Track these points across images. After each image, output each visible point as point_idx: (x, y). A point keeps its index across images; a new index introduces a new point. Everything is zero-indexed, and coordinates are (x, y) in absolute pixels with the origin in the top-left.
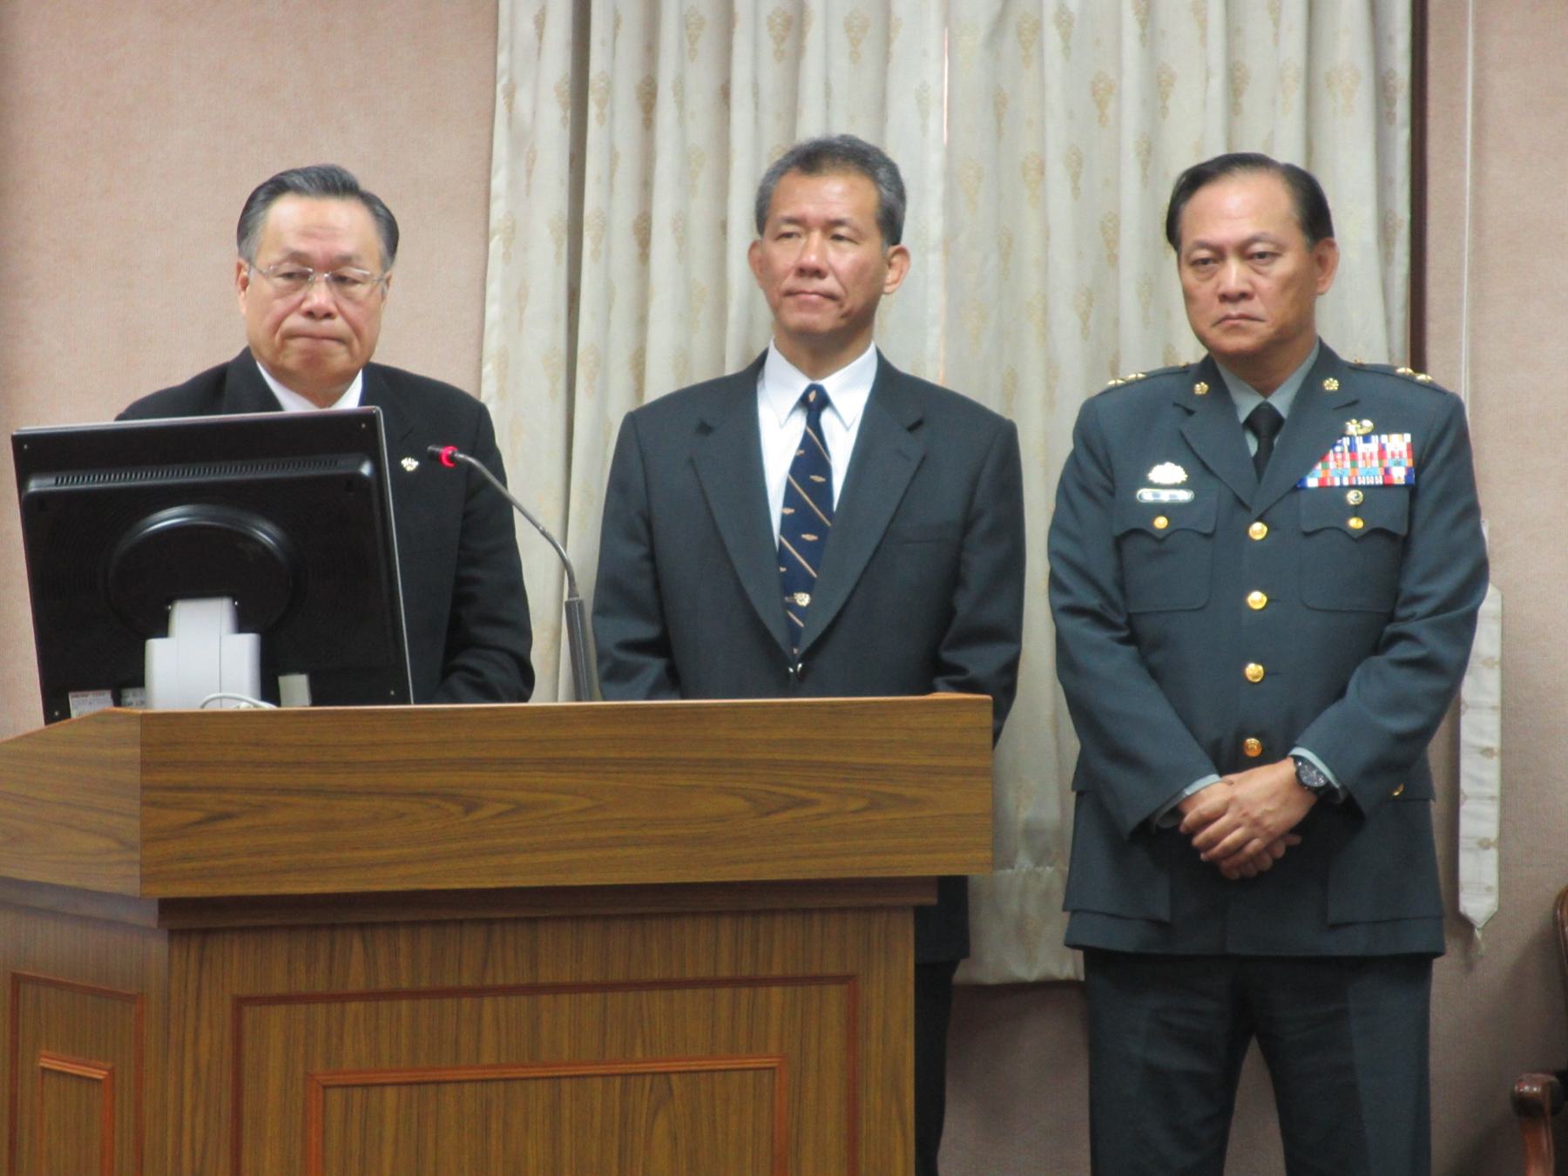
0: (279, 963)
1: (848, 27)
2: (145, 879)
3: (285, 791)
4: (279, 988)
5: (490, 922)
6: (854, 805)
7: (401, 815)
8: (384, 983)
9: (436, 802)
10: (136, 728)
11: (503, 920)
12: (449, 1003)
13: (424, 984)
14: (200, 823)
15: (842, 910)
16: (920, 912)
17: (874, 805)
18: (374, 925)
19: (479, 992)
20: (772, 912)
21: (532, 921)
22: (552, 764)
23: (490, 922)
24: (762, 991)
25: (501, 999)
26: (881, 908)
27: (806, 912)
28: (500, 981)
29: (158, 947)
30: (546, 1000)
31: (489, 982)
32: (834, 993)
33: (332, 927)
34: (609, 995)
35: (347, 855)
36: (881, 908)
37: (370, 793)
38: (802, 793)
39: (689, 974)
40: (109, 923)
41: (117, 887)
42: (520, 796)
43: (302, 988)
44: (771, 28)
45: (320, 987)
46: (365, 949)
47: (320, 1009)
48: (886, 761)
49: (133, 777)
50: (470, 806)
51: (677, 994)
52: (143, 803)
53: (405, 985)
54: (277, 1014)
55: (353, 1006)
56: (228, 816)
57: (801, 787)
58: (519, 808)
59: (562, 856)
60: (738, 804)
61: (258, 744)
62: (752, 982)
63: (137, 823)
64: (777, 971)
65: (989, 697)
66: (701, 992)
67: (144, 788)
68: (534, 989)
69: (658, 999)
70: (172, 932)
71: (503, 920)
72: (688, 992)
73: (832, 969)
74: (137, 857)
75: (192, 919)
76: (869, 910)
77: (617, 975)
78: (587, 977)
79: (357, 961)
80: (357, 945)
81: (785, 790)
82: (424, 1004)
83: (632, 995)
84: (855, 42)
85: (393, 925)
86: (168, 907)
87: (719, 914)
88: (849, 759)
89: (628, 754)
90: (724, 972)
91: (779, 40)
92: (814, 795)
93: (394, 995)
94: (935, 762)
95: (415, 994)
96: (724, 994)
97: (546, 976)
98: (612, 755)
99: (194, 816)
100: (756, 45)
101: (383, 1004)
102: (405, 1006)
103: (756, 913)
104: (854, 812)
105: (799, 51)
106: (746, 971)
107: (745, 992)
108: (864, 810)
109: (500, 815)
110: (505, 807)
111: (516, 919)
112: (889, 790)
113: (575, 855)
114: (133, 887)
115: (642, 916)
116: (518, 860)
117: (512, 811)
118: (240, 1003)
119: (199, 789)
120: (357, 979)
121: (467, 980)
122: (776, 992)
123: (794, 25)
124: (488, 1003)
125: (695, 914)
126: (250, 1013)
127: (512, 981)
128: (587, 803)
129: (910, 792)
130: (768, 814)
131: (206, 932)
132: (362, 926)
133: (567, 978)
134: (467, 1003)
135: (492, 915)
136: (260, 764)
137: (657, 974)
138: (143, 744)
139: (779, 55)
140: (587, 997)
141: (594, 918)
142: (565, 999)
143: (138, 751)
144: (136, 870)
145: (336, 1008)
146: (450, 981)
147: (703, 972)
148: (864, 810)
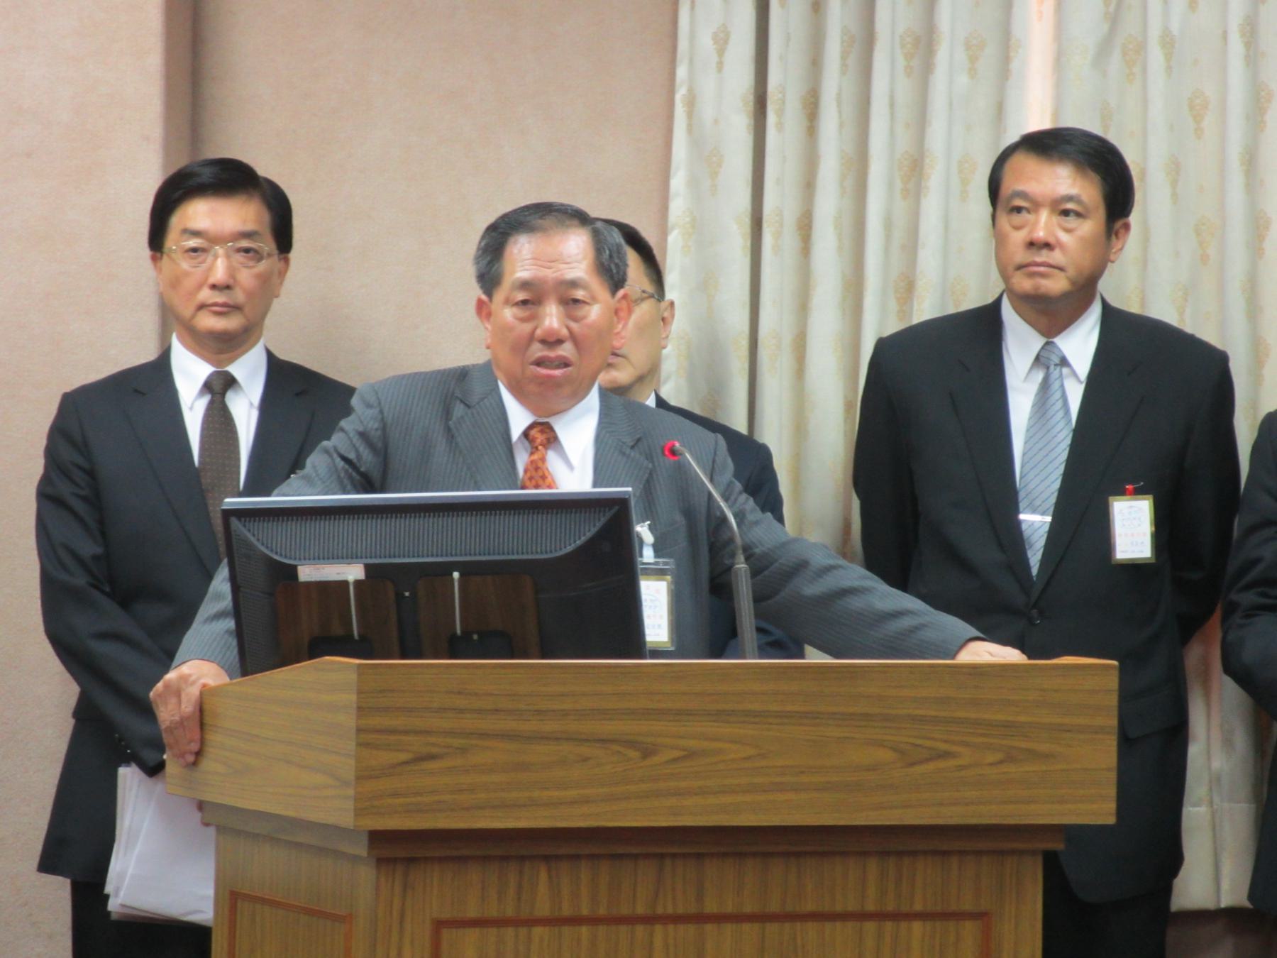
0: (473, 891)
1: (968, 46)
2: (359, 813)
3: (484, 735)
4: (472, 912)
5: (662, 856)
6: (991, 758)
7: (586, 759)
8: (566, 911)
9: (615, 747)
10: (353, 677)
11: (674, 856)
12: (624, 929)
13: (602, 911)
14: (406, 763)
15: (979, 853)
16: (1051, 862)
17: (1010, 758)
18: (558, 858)
19: (650, 920)
20: (914, 854)
21: (699, 856)
22: (721, 716)
23: (662, 856)
24: (904, 925)
25: (671, 927)
26: (1013, 852)
27: (945, 853)
28: (670, 910)
29: (366, 875)
30: (709, 927)
31: (660, 911)
32: (969, 929)
33: (522, 859)
34: (768, 925)
35: (536, 794)
36: (1013, 852)
37: (557, 739)
38: (943, 747)
39: (839, 908)
40: (321, 851)
41: (331, 819)
42: (692, 744)
43: (493, 912)
44: (903, 46)
45: (510, 912)
46: (550, 877)
47: (510, 932)
48: (1022, 718)
49: (349, 721)
50: (647, 752)
51: (828, 926)
52: (359, 744)
53: (585, 912)
54: (472, 935)
55: (538, 931)
56: (431, 757)
57: (946, 741)
58: (691, 755)
59: (728, 799)
60: (886, 755)
61: (459, 693)
62: (896, 916)
63: (352, 762)
64: (918, 907)
65: (1115, 663)
66: (851, 926)
67: (359, 730)
68: (701, 918)
69: (811, 928)
70: (381, 862)
71: (674, 856)
72: (838, 924)
73: (967, 906)
74: (351, 792)
75: (399, 850)
76: (1002, 853)
77: (774, 906)
78: (748, 909)
79: (544, 890)
80: (543, 875)
81: (928, 743)
82: (602, 930)
83: (787, 925)
84: (973, 59)
85: (576, 858)
86: (378, 838)
87: (865, 854)
88: (986, 716)
89: (789, 708)
90: (871, 907)
91: (909, 56)
92: (954, 748)
93: (576, 921)
94: (1067, 720)
95: (594, 921)
96: (870, 926)
97: (711, 907)
98: (775, 708)
99: (403, 757)
100: (893, 62)
101: (566, 930)
102: (584, 930)
103: (900, 854)
104: (991, 764)
105: (928, 67)
106: (890, 907)
107: (889, 926)
108: (1001, 762)
109: (675, 760)
110: (677, 754)
111: (684, 856)
112: (1023, 745)
113: (740, 798)
114: (347, 820)
115: (798, 855)
116: (689, 802)
117: (684, 757)
118: (440, 925)
119: (406, 732)
120: (543, 908)
121: (640, 910)
122: (917, 926)
123: (923, 45)
124: (658, 928)
125: (844, 854)
126: (446, 934)
127: (680, 910)
128: (752, 752)
129: (1044, 747)
130: (912, 764)
131: (411, 861)
132: (547, 858)
133: (729, 908)
134: (640, 930)
135: (664, 850)
136: (461, 711)
137: (810, 907)
138: (360, 692)
139: (908, 70)
140: (746, 927)
141: (754, 855)
142: (728, 928)
143: (354, 697)
144: (350, 805)
145: (523, 931)
146: (625, 910)
147: (852, 906)
148: (1001, 762)
